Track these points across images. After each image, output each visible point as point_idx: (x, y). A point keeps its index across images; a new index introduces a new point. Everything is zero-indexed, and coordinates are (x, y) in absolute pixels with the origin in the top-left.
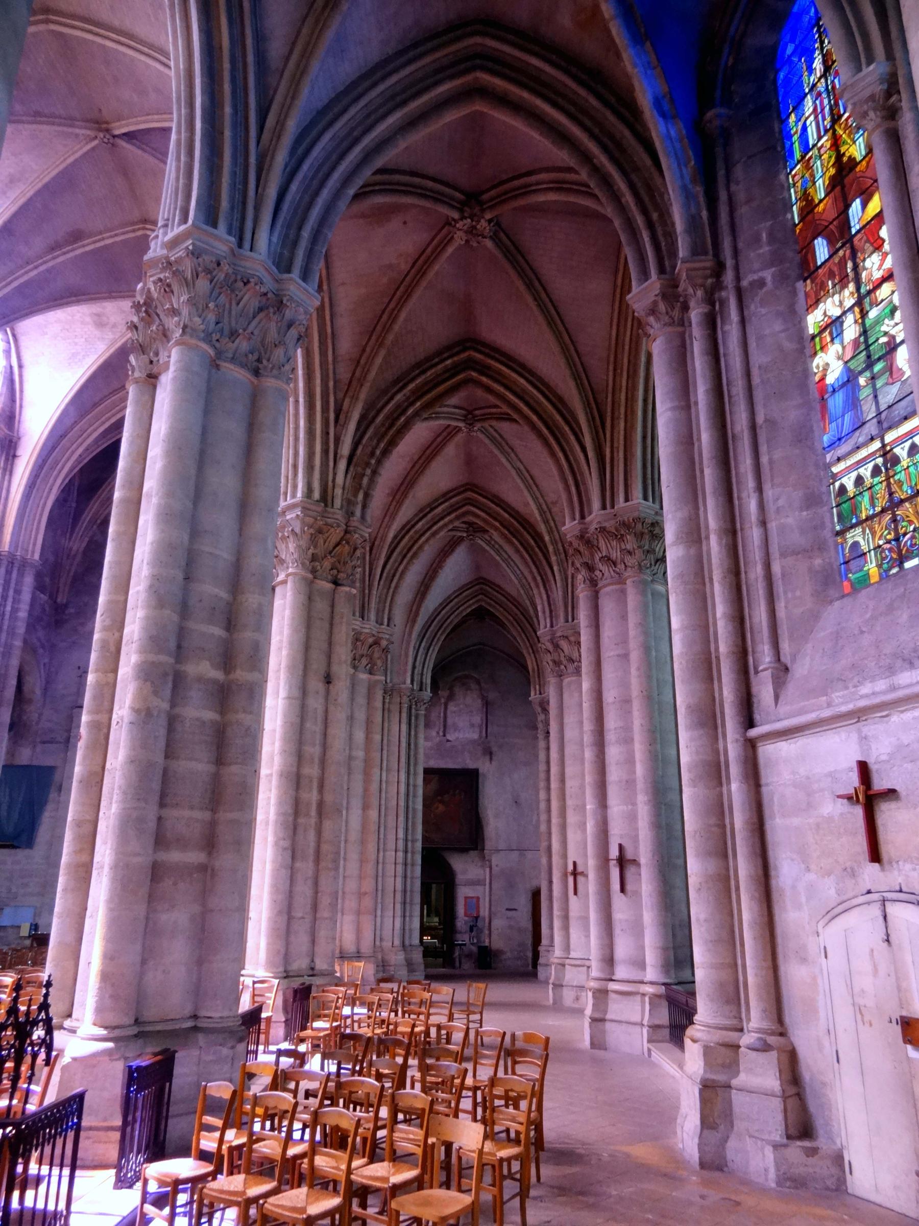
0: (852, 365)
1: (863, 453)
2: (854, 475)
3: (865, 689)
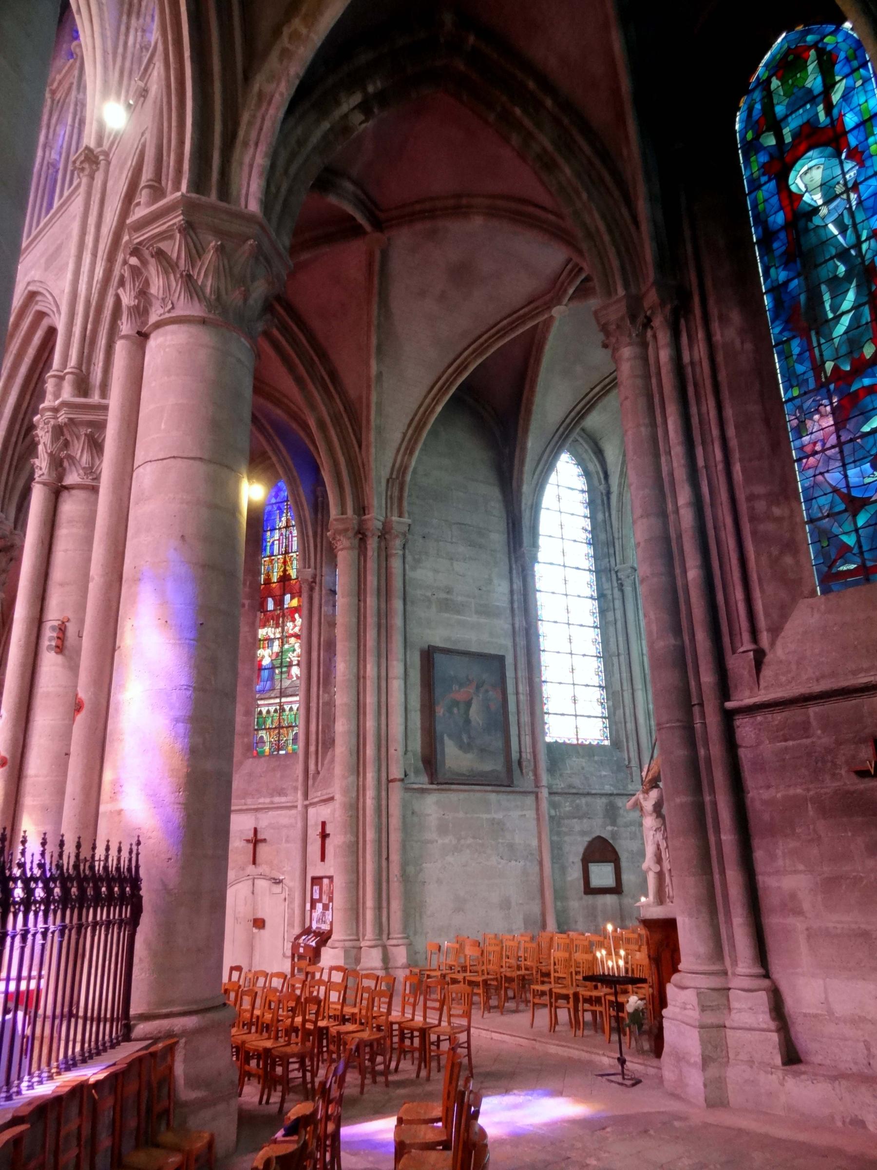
0: (275, 662)
1: (272, 701)
2: (267, 708)
3: (261, 800)
